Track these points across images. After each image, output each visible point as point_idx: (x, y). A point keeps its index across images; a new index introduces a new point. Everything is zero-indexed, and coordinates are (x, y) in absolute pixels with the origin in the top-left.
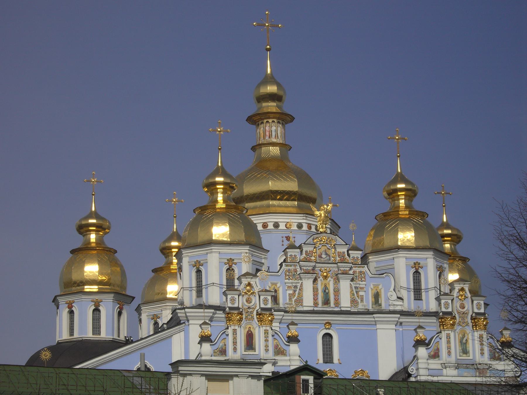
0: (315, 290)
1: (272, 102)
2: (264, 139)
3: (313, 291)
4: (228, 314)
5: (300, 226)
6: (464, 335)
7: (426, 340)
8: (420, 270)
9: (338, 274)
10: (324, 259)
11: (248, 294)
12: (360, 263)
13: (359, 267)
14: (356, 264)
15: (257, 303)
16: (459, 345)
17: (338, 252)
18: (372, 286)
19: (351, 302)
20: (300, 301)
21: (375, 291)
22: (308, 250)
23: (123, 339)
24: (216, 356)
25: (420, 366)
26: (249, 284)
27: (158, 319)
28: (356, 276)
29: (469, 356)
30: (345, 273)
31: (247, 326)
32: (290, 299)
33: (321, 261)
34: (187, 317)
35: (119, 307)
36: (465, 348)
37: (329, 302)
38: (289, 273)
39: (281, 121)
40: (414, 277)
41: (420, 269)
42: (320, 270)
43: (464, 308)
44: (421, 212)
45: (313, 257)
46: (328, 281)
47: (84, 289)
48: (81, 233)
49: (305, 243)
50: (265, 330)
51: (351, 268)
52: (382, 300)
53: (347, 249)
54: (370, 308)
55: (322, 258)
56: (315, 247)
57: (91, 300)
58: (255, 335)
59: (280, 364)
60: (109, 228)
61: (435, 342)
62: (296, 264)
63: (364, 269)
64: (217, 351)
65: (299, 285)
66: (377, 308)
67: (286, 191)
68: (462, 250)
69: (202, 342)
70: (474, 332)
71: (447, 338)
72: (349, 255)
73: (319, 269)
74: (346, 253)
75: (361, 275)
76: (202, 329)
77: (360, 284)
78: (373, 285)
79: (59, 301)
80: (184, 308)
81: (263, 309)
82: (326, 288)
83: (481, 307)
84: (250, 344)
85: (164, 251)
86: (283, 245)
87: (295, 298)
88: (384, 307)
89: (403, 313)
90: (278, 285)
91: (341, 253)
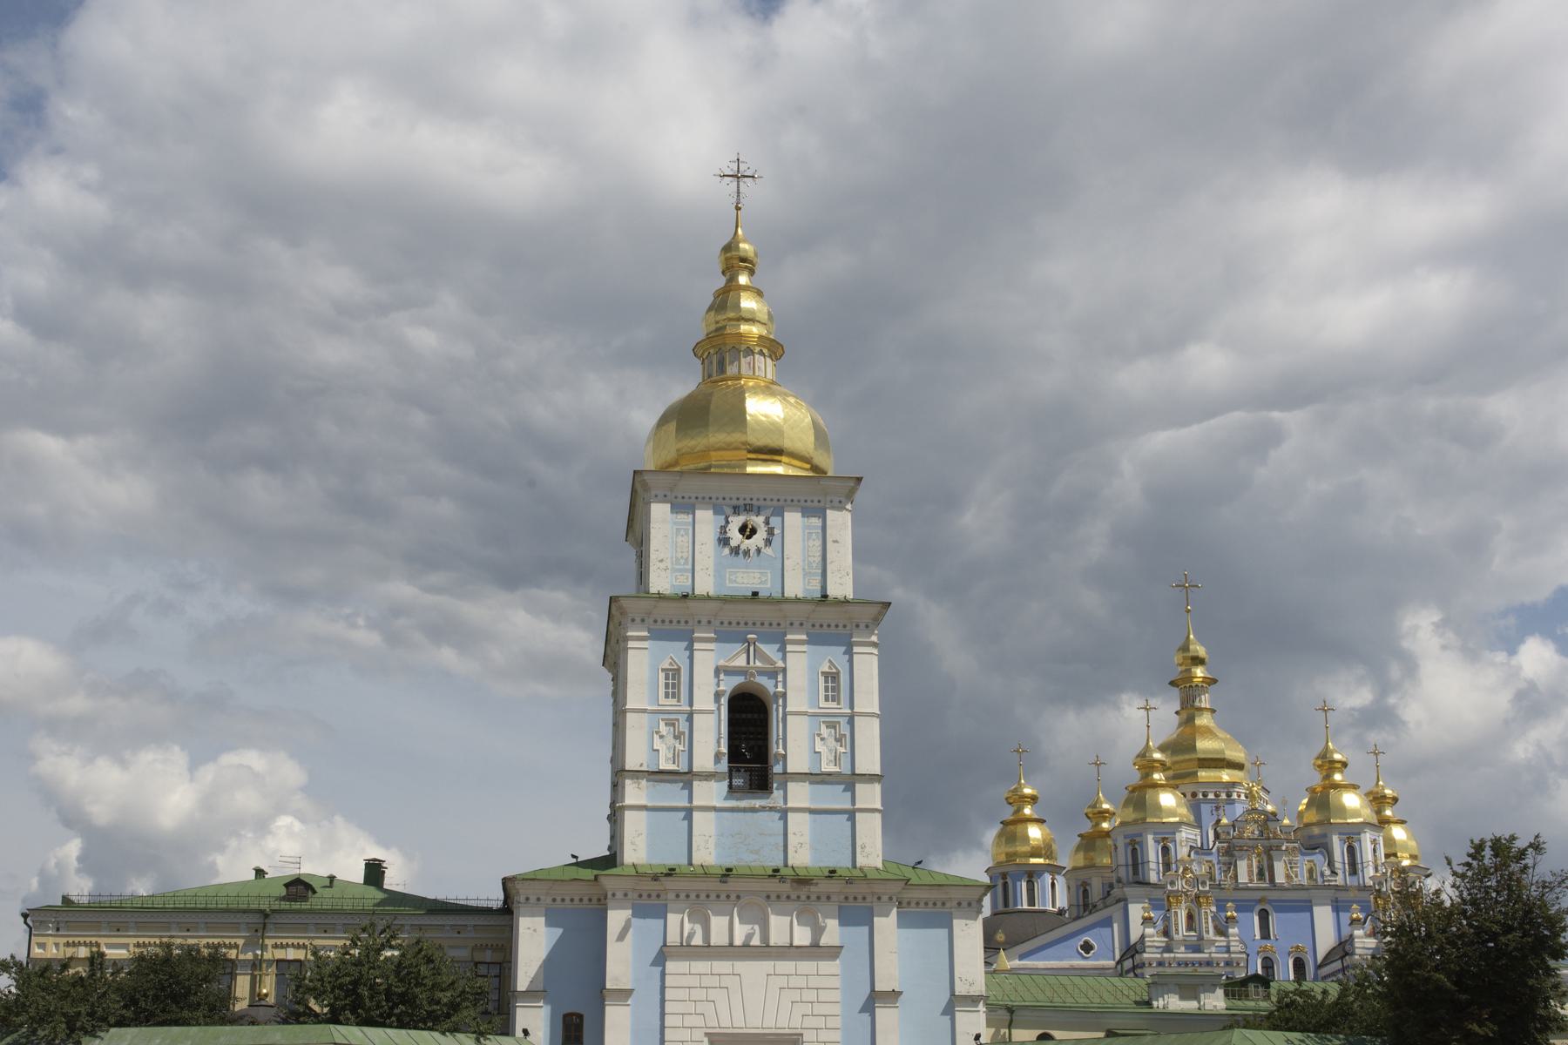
0: (1250, 866)
5: (1229, 795)
8: (1356, 845)
21: (1309, 866)
25: (1357, 945)
39: (1204, 685)
48: (1010, 804)
54: (1305, 882)
66: (1313, 883)
84: (1190, 927)
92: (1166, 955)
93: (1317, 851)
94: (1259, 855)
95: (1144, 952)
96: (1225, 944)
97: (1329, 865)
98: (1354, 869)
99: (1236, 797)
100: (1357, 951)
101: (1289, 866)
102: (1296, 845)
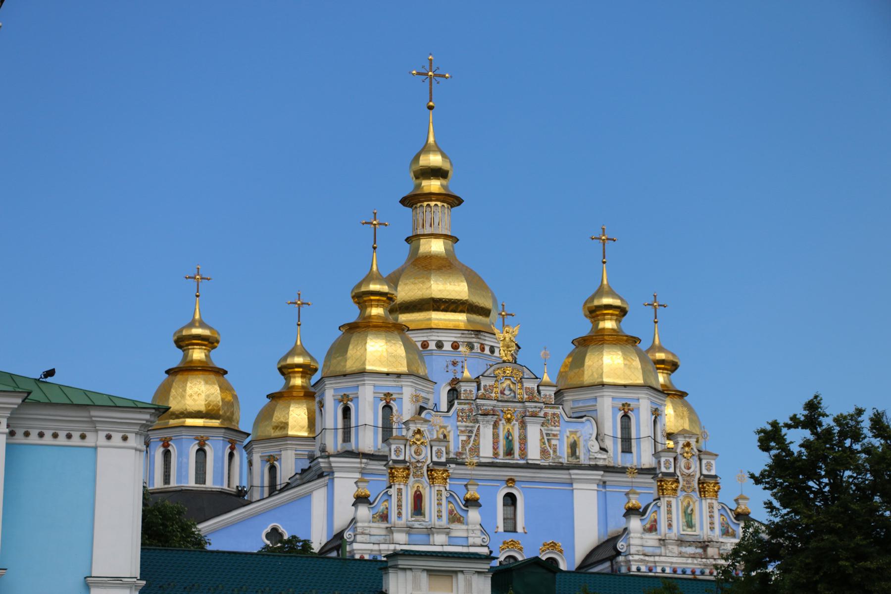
0: (496, 437)
1: (435, 179)
2: (423, 227)
3: (493, 438)
4: (392, 469)
5: (471, 346)
6: (689, 504)
7: (640, 508)
8: (630, 414)
9: (525, 416)
10: (508, 397)
11: (416, 443)
12: (553, 403)
13: (553, 408)
14: (548, 404)
15: (427, 456)
16: (682, 516)
17: (526, 388)
18: (568, 434)
19: (541, 453)
20: (476, 450)
21: (571, 440)
22: (488, 384)
23: (235, 490)
24: (375, 522)
25: (632, 542)
26: (419, 432)
27: (275, 462)
28: (548, 420)
29: (695, 531)
30: (534, 415)
31: (415, 485)
32: (463, 447)
33: (504, 398)
34: (331, 467)
35: (231, 448)
36: (690, 520)
37: (512, 452)
38: (462, 413)
39: (445, 205)
40: (622, 422)
41: (630, 412)
42: (502, 411)
43: (689, 468)
44: (632, 337)
45: (494, 392)
46: (512, 424)
47: (185, 421)
48: (180, 347)
49: (485, 375)
50: (437, 491)
51: (541, 409)
52: (581, 452)
53: (536, 385)
54: (564, 460)
55: (504, 394)
56: (497, 381)
57: (194, 437)
58: (425, 496)
59: (453, 534)
60: (218, 342)
61: (654, 510)
62: (471, 402)
63: (559, 410)
64: (377, 516)
65: (475, 429)
66: (574, 461)
67: (452, 299)
68: (679, 381)
69: (359, 504)
70: (702, 499)
71: (667, 507)
72: (539, 392)
73: (501, 409)
74: (536, 389)
75: (554, 418)
76: (359, 488)
77: (552, 430)
78: (570, 431)
79: (151, 438)
80: (329, 456)
81: (435, 463)
82: (508, 434)
83: (711, 468)
85: (284, 370)
86: (447, 371)
87: (470, 445)
88: (584, 460)
89: (607, 470)
90: (448, 429)
91: (529, 388)
92: (383, 547)
93: (584, 419)
94: (509, 421)
95: (354, 541)
96: (464, 534)
97: (597, 439)
98: (627, 445)
99: (479, 351)
100: (633, 550)
101: (546, 438)
102: (559, 411)
